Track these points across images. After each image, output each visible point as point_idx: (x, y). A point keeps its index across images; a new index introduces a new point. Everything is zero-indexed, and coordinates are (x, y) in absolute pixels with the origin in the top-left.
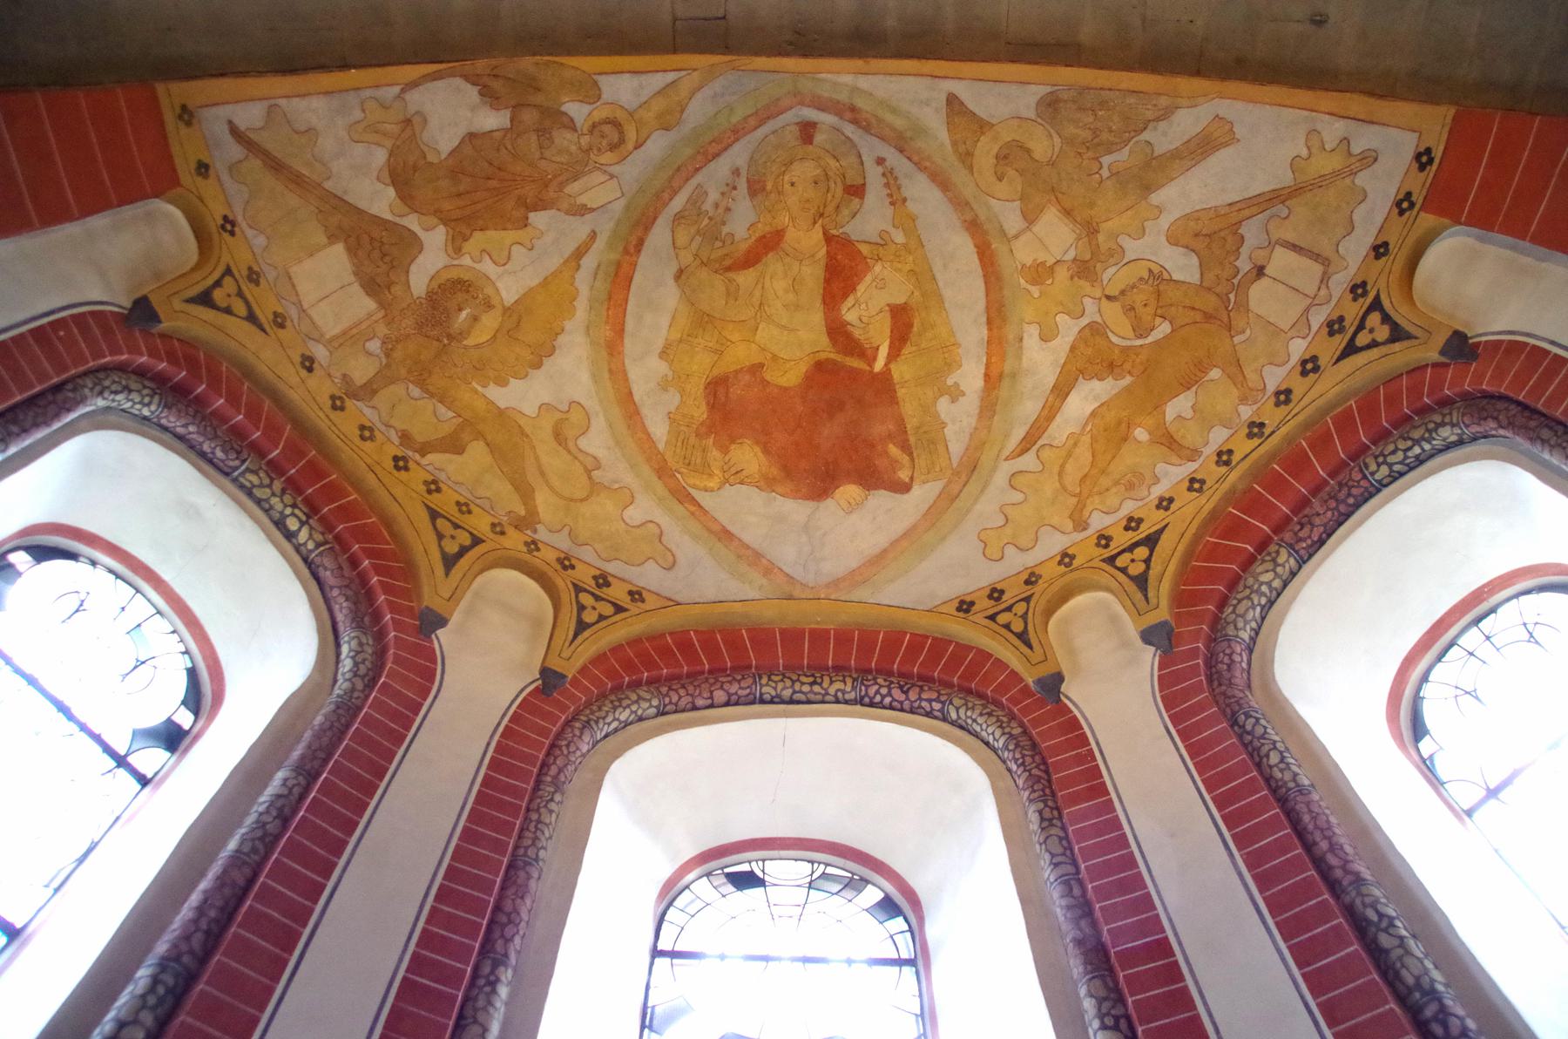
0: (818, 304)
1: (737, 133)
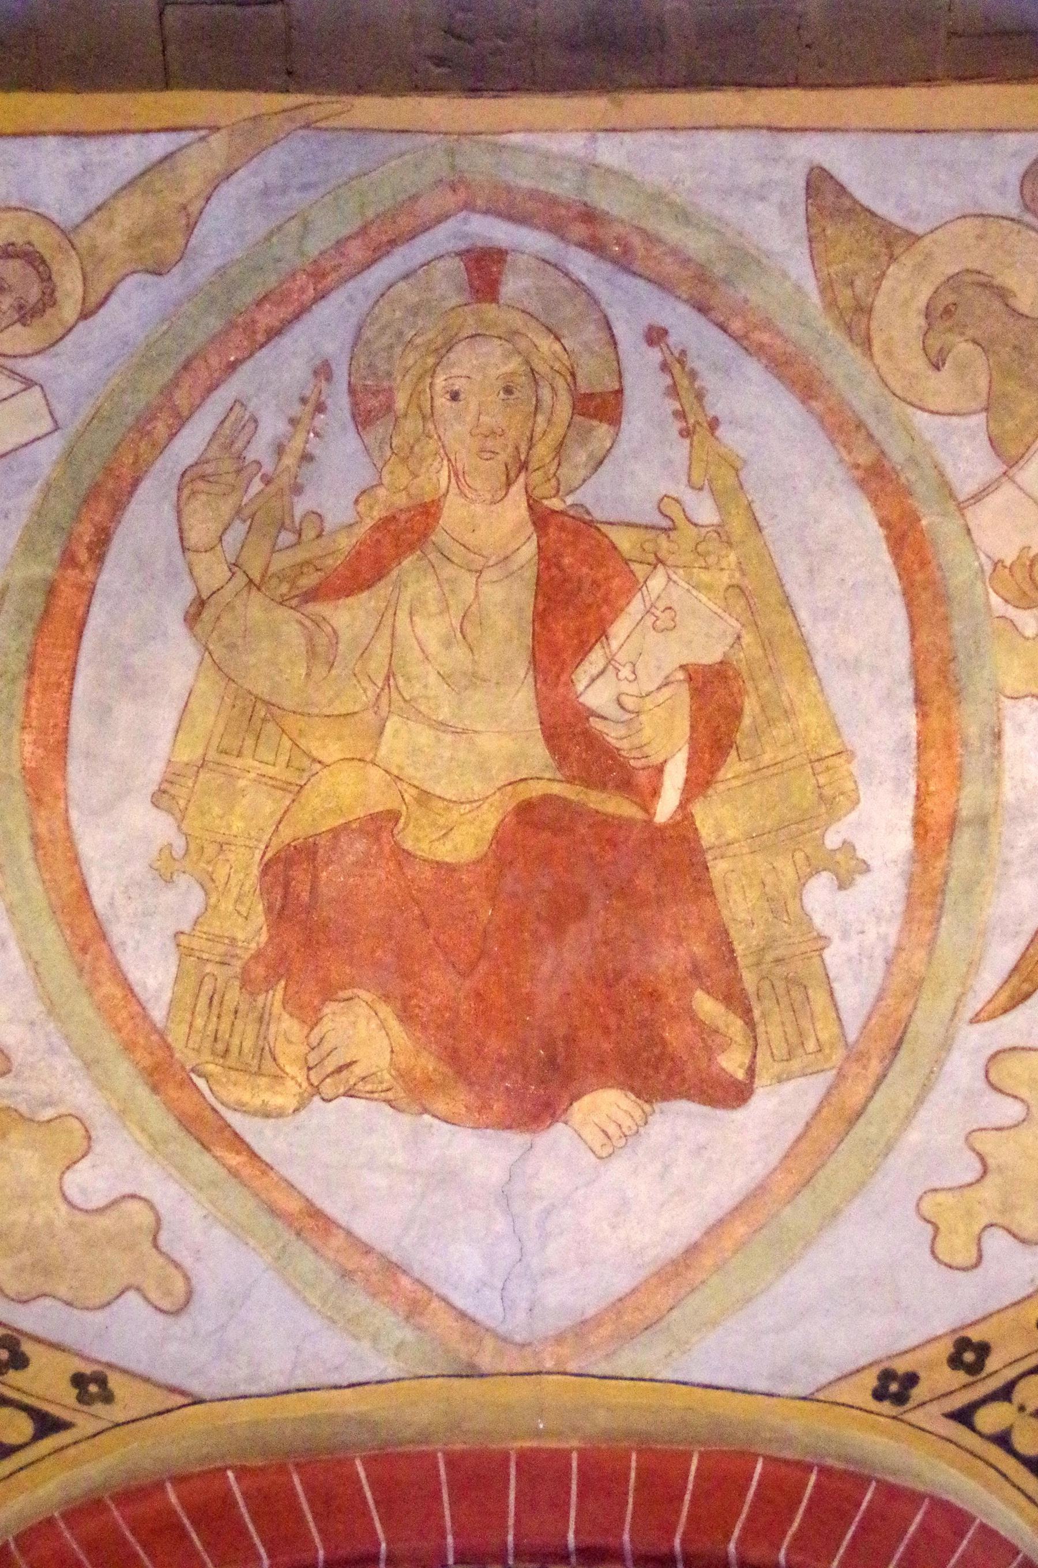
0: (521, 669)
1: (321, 279)
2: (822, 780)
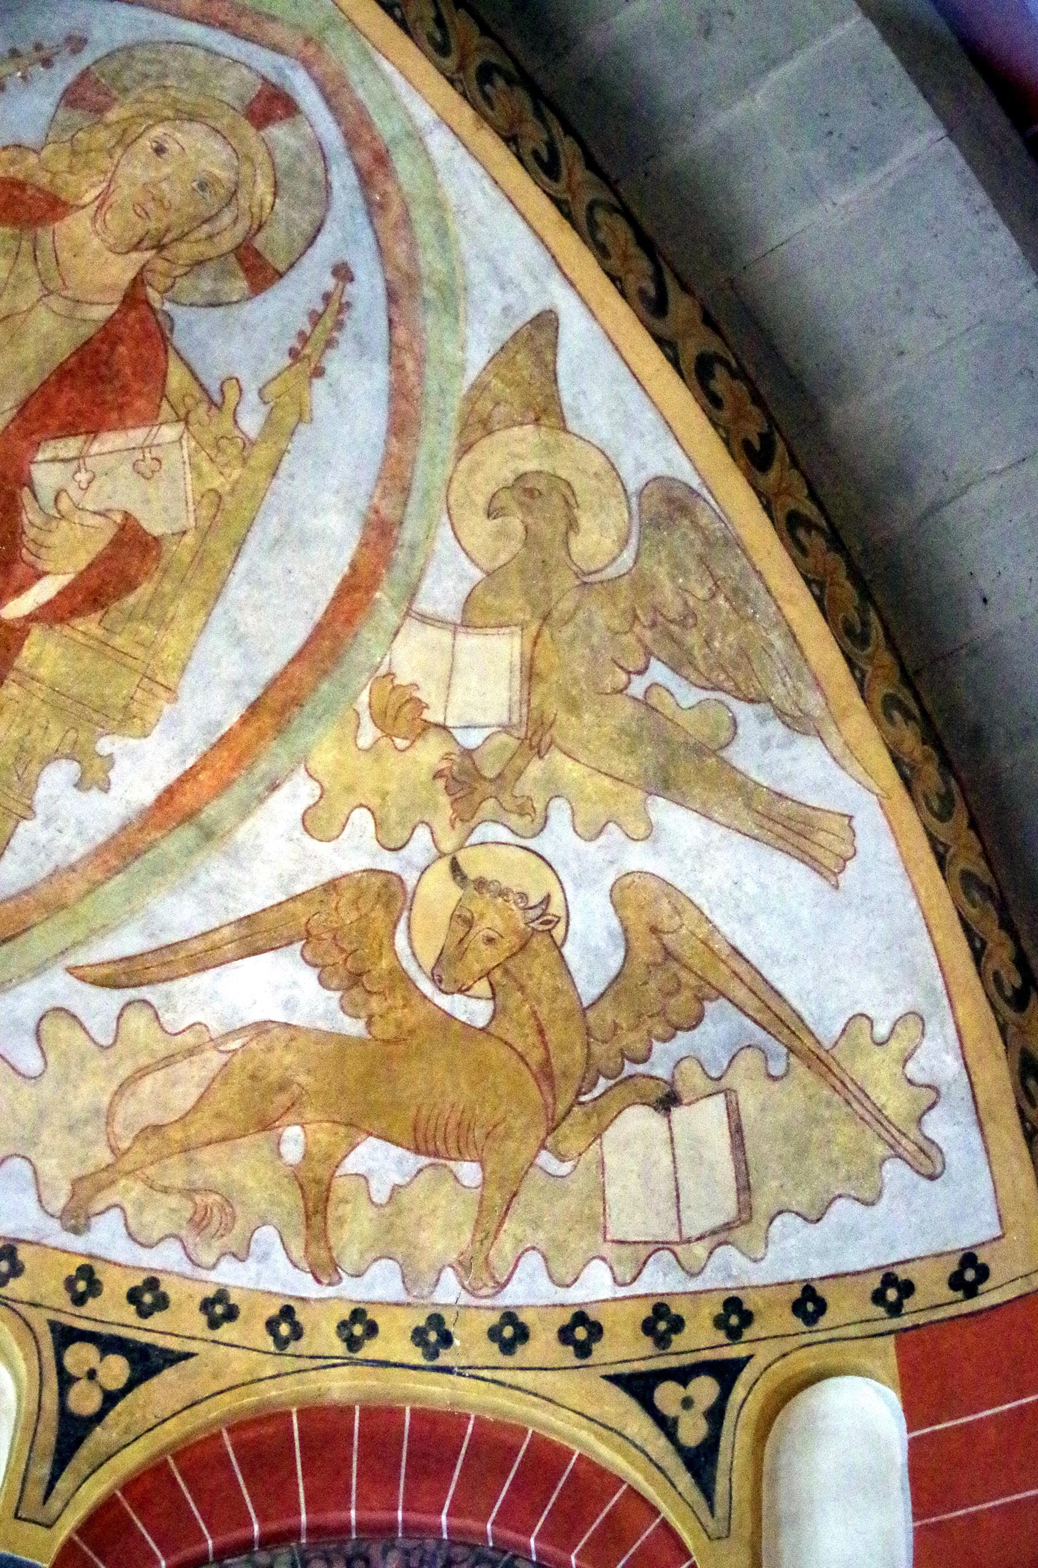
2: (139, 695)
